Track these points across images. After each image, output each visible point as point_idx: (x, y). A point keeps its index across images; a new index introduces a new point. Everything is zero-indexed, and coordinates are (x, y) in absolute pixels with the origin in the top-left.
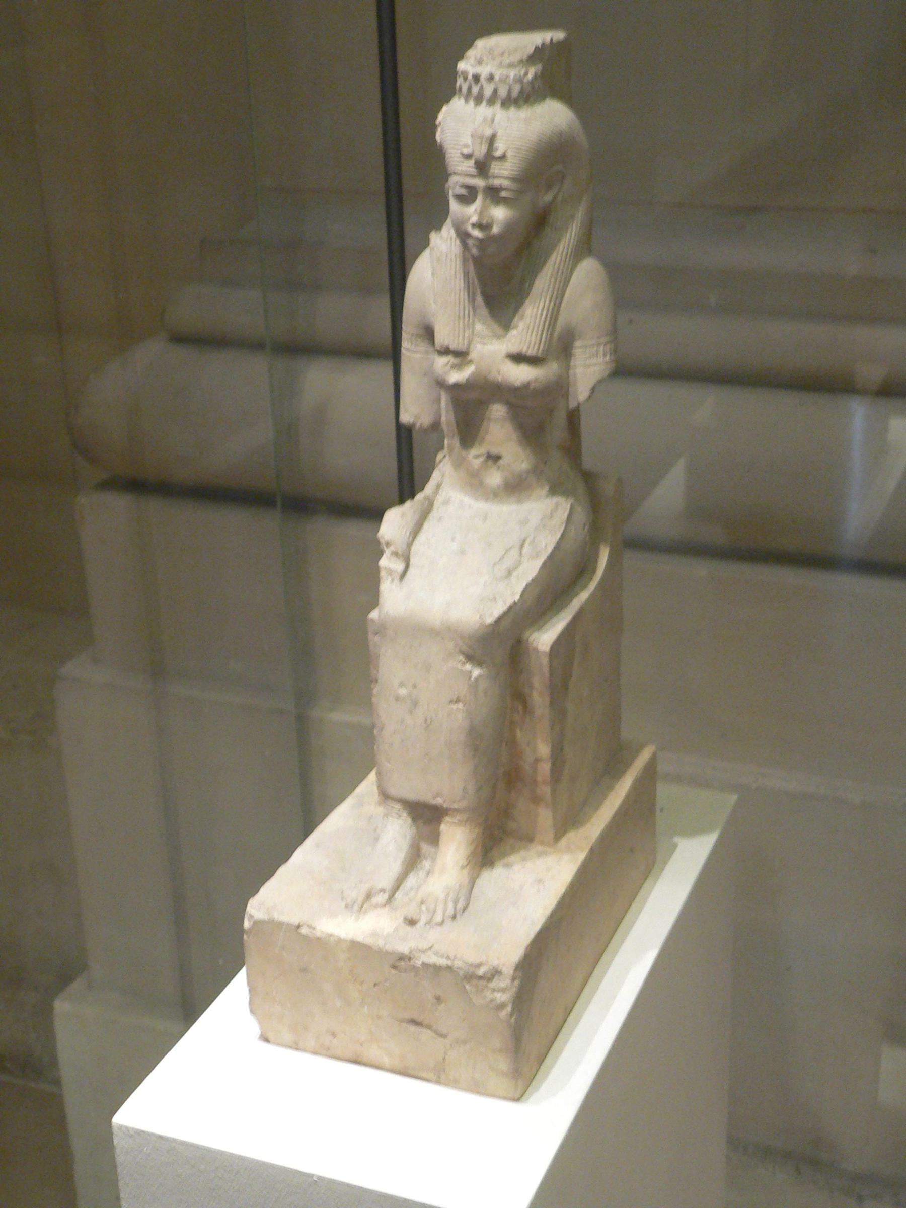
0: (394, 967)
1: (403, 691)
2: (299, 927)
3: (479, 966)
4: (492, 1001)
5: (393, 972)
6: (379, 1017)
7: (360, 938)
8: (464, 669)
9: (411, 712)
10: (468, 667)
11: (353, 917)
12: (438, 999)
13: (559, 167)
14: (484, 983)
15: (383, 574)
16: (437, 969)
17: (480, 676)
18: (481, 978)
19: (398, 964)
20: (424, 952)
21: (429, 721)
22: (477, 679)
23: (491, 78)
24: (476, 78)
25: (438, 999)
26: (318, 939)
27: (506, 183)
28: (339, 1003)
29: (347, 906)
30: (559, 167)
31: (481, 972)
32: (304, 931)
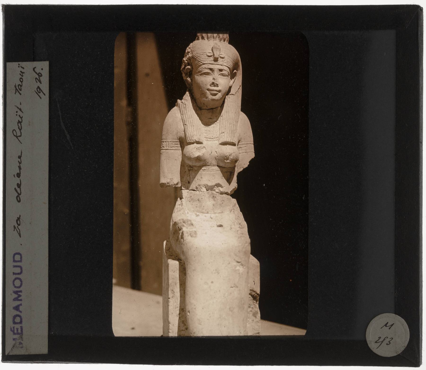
10: (238, 268)
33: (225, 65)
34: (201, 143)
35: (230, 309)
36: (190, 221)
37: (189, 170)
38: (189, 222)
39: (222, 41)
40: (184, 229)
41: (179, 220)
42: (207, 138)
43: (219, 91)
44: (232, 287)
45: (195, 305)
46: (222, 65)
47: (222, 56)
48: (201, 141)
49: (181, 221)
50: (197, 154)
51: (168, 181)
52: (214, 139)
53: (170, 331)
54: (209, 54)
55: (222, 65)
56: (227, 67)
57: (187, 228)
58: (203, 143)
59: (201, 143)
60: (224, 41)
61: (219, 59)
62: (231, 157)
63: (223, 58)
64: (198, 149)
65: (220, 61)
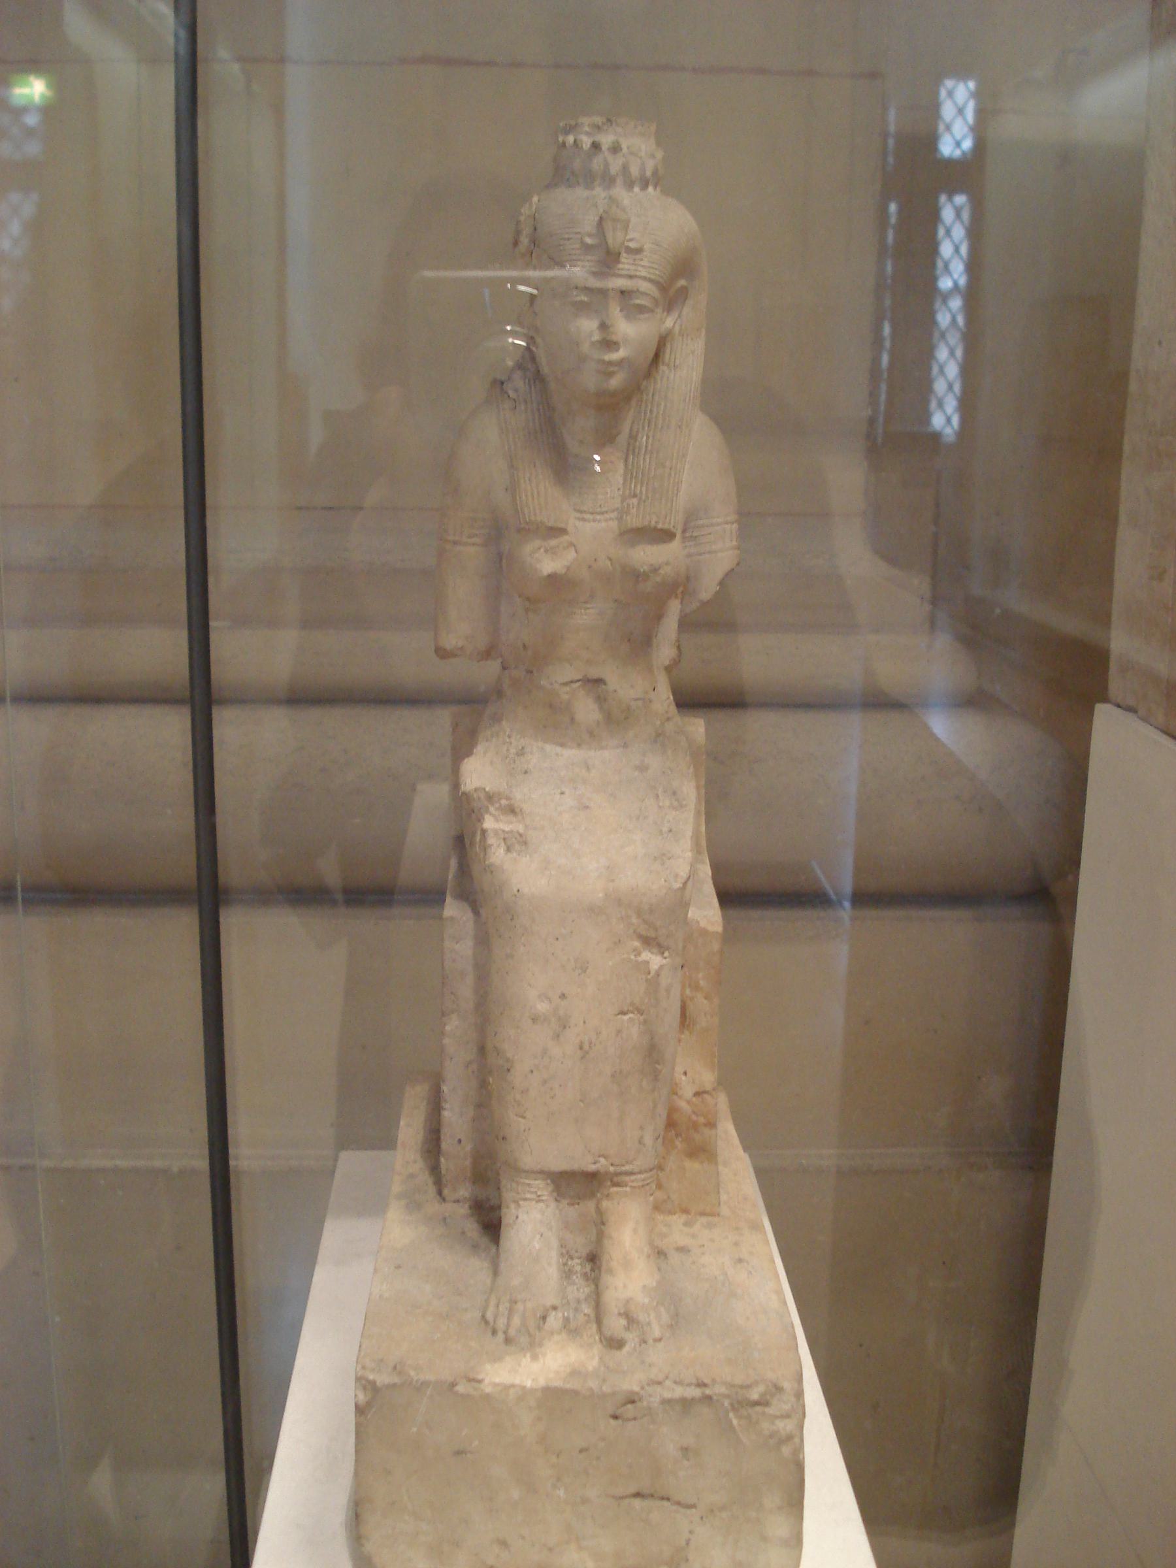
0: (615, 1417)
1: (542, 1007)
2: (453, 1385)
3: (748, 1387)
4: (771, 1436)
5: (613, 1422)
6: (585, 1501)
7: (558, 1383)
8: (640, 959)
9: (557, 1036)
10: (646, 955)
11: (528, 1355)
12: (685, 1450)
13: (682, 282)
14: (758, 1409)
15: (491, 840)
16: (686, 1404)
17: (661, 967)
18: (757, 1403)
19: (619, 1412)
20: (659, 1383)
21: (586, 1047)
22: (658, 975)
23: (615, 149)
24: (596, 146)
25: (685, 1450)
26: (487, 1397)
27: (645, 286)
28: (516, 1494)
29: (508, 1341)
30: (682, 282)
31: (755, 1395)
32: (460, 1388)
33: (643, 273)
34: (563, 531)
35: (613, 1076)
36: (508, 798)
37: (527, 610)
38: (504, 802)
39: (636, 189)
40: (489, 823)
41: (476, 790)
42: (581, 512)
43: (620, 363)
44: (623, 1013)
45: (508, 1060)
46: (631, 277)
47: (632, 245)
48: (562, 525)
49: (482, 795)
50: (548, 565)
51: (460, 644)
52: (607, 516)
53: (447, 1106)
54: (589, 241)
55: (631, 277)
56: (650, 281)
57: (497, 820)
58: (570, 528)
59: (563, 531)
60: (645, 187)
61: (624, 255)
62: (658, 579)
63: (639, 251)
64: (552, 552)
65: (626, 264)
